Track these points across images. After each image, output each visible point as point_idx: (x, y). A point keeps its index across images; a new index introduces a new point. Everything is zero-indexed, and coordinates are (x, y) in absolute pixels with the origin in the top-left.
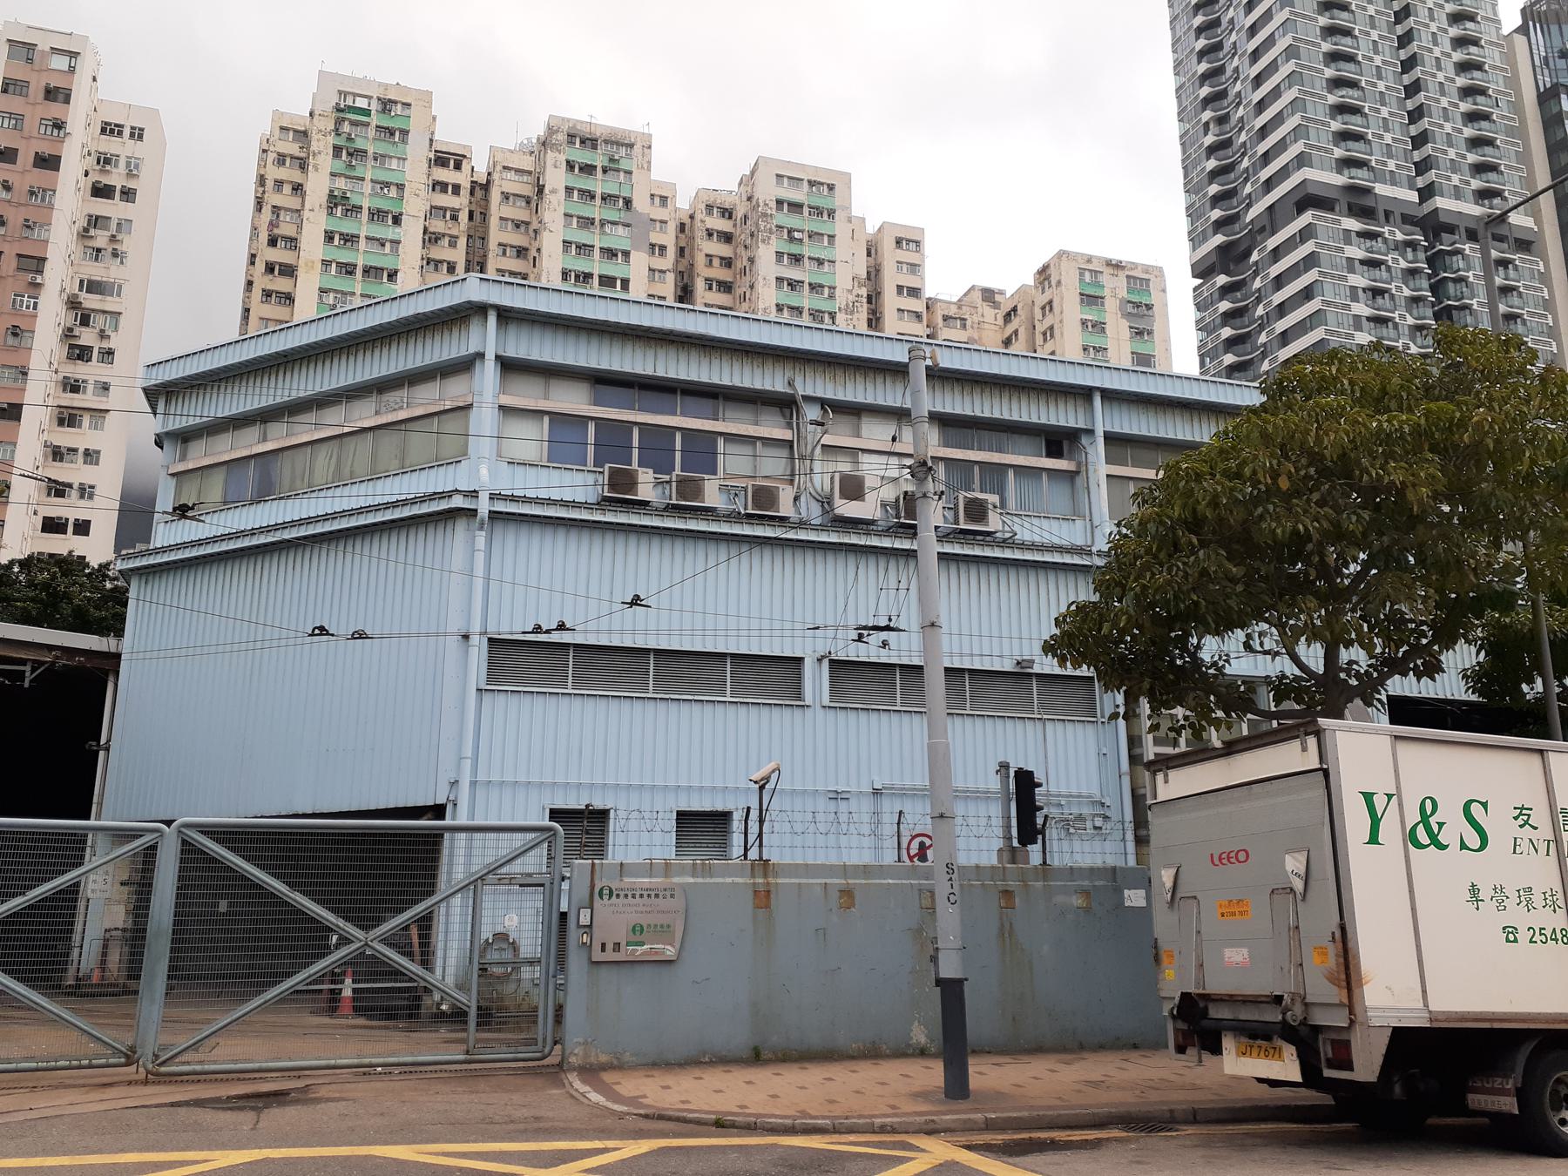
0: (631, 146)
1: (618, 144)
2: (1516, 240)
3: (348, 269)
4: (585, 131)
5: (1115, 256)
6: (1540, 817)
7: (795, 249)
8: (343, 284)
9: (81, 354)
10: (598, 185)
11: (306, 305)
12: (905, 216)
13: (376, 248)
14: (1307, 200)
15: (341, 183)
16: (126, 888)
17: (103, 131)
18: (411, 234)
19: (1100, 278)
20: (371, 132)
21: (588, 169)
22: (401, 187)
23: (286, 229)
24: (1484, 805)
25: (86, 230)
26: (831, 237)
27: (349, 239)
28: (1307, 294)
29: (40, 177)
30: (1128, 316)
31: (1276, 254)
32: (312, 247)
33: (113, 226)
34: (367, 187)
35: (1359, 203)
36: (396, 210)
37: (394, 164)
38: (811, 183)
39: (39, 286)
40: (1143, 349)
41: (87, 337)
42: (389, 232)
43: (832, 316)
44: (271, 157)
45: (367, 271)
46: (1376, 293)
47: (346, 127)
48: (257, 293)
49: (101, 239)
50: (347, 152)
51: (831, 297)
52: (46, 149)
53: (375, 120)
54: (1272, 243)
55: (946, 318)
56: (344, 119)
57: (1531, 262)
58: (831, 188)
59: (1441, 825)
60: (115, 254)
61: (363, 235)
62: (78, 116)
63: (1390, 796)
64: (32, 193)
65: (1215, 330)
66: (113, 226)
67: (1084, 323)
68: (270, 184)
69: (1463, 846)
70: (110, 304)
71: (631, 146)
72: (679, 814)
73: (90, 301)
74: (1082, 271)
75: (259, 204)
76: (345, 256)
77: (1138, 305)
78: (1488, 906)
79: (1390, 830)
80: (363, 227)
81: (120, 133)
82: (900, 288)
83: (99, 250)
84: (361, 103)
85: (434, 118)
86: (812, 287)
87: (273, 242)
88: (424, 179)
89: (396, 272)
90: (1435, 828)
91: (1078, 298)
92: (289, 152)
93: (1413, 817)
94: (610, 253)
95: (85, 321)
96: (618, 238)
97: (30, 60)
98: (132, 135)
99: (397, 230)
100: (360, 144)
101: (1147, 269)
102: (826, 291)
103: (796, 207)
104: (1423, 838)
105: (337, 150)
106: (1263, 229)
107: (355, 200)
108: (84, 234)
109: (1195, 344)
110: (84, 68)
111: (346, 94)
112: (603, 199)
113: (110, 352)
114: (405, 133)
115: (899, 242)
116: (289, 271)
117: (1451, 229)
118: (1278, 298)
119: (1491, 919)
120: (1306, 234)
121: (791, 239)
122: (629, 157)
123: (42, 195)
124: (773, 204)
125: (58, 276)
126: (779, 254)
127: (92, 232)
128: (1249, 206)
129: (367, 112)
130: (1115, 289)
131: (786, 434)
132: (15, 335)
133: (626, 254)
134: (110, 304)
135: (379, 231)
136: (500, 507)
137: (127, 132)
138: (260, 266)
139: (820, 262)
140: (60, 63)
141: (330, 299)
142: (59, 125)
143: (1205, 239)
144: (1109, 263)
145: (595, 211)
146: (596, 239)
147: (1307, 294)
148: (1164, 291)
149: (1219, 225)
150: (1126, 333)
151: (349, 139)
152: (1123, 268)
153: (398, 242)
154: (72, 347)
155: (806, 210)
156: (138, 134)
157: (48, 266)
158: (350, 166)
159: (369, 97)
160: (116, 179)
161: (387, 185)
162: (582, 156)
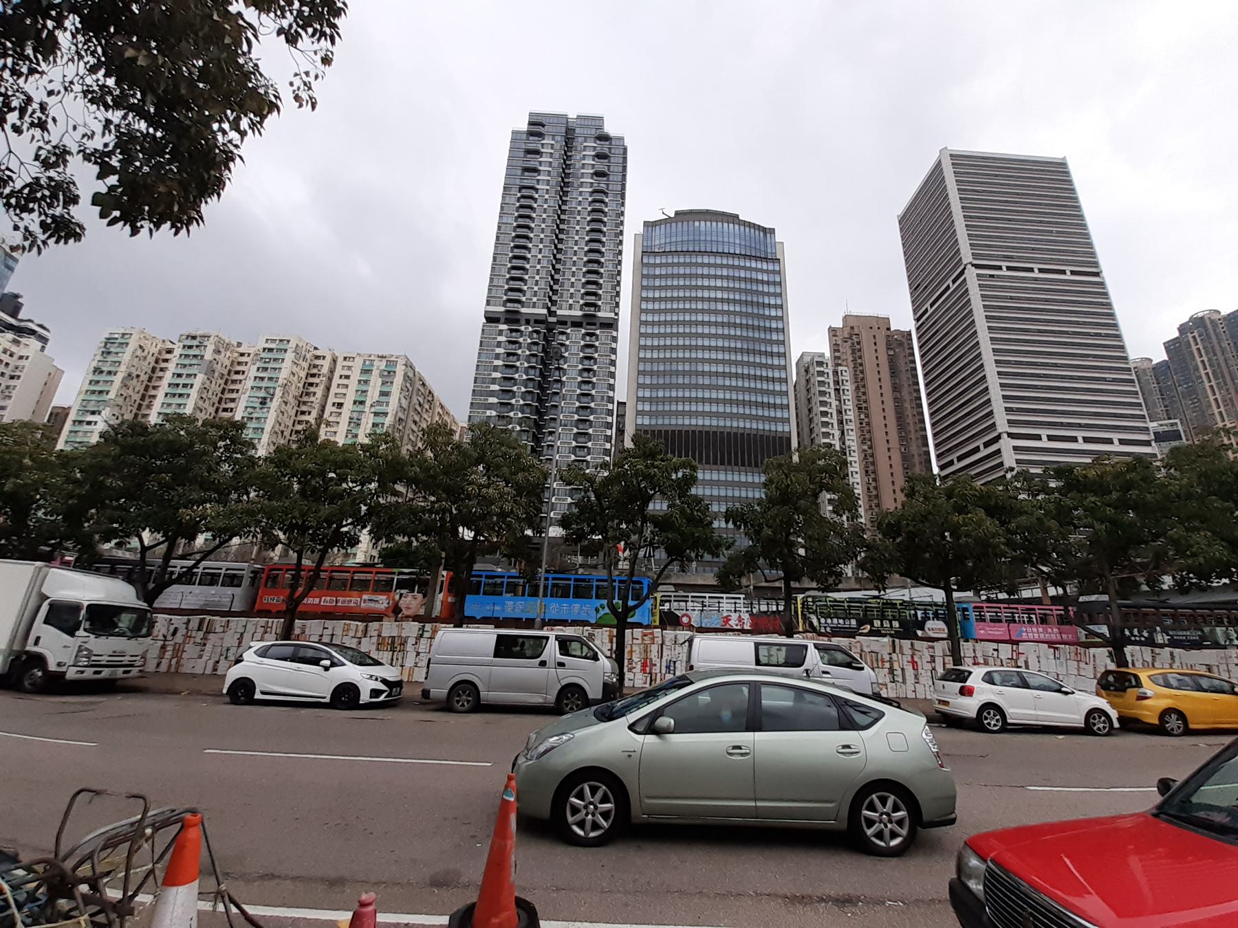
10: (191, 352)
21: (190, 347)
30: (381, 376)
35: (512, 318)
46: (509, 354)
86: (270, 379)
94: (189, 376)
103: (271, 350)
115: (345, 359)
117: (565, 323)
145: (187, 362)
162: (189, 342)
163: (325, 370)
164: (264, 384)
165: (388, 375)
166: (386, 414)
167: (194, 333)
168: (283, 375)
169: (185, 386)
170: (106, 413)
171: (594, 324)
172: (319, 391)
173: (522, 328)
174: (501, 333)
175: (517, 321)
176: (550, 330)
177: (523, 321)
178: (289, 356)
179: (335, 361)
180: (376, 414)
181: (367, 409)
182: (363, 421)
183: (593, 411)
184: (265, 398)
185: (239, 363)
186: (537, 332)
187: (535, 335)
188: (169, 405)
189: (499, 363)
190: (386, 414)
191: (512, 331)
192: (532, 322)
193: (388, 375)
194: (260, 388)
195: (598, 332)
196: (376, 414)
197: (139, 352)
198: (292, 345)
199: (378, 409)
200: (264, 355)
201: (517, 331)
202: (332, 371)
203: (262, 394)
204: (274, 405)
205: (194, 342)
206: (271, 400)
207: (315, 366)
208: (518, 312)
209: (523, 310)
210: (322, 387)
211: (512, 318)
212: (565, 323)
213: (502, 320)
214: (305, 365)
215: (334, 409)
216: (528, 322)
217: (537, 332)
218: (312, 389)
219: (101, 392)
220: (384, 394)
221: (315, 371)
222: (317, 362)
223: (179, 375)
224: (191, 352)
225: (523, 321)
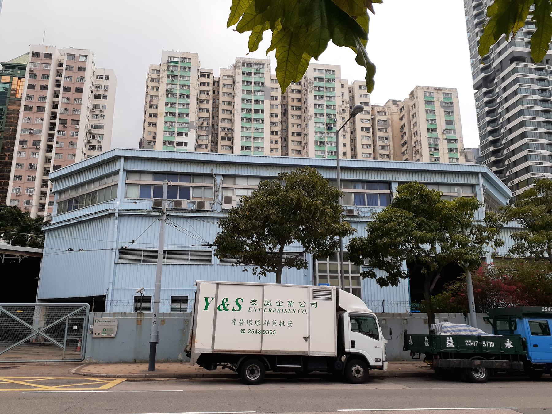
0: (264, 64)
1: (259, 64)
3: (173, 114)
4: (248, 61)
5: (438, 86)
6: (259, 303)
7: (321, 94)
8: (172, 119)
9: (92, 148)
10: (253, 79)
11: (79, 157)
13: (181, 107)
14: (514, 58)
15: (170, 86)
16: (44, 317)
17: (97, 78)
18: (193, 101)
19: (433, 94)
20: (179, 69)
21: (249, 74)
22: (189, 86)
23: (154, 102)
24: (242, 300)
25: (93, 109)
26: (334, 88)
27: (173, 104)
28: (515, 93)
29: (77, 95)
30: (443, 107)
31: (504, 79)
32: (162, 108)
33: (101, 107)
34: (178, 87)
36: (187, 94)
37: (187, 79)
38: (326, 70)
39: (78, 129)
40: (450, 119)
41: (94, 143)
42: (185, 101)
43: (335, 115)
44: (150, 79)
45: (179, 114)
46: (543, 90)
47: (171, 68)
48: (147, 124)
49: (97, 112)
50: (172, 76)
51: (334, 109)
52: (79, 86)
53: (180, 65)
54: (502, 75)
55: (378, 112)
56: (170, 65)
58: (333, 71)
59: (228, 305)
60: (102, 116)
61: (177, 103)
62: (88, 74)
63: (213, 298)
64: (75, 100)
65: (482, 108)
66: (101, 107)
67: (427, 111)
68: (150, 88)
69: (233, 310)
70: (100, 132)
71: (264, 64)
72: (172, 297)
73: (95, 131)
74: (425, 92)
75: (147, 94)
76: (172, 110)
77: (447, 103)
78: (238, 324)
79: (212, 306)
80: (177, 100)
81: (102, 78)
83: (97, 115)
84: (176, 60)
85: (200, 62)
86: (328, 106)
87: (151, 107)
88: (196, 82)
89: (188, 114)
90: (226, 306)
91: (424, 102)
92: (154, 79)
93: (220, 302)
94: (257, 102)
95: (93, 138)
96: (260, 96)
97: (73, 59)
98: (106, 78)
99: (188, 100)
100: (175, 73)
101: (450, 90)
102: (332, 107)
103: (321, 79)
104: (222, 308)
105: (168, 76)
106: (498, 70)
107: (174, 91)
108: (92, 111)
109: (476, 114)
110: (90, 59)
111: (171, 57)
112: (255, 83)
113: (101, 147)
114: (189, 68)
116: (155, 116)
118: (505, 95)
119: (238, 327)
120: (514, 71)
121: (320, 90)
122: (263, 68)
123: (78, 100)
124: (313, 79)
125: (84, 126)
126: (315, 96)
127: (95, 110)
128: (493, 62)
129: (177, 63)
130: (438, 98)
131: (212, 185)
132: (72, 144)
133: (263, 101)
134: (100, 132)
135: (183, 101)
136: (122, 212)
137: (104, 77)
138: (147, 115)
139: (330, 97)
140: (82, 59)
141: (168, 124)
142: (82, 78)
143: (478, 75)
144: (435, 89)
145: (252, 88)
146: (252, 97)
147: (515, 93)
148: (457, 97)
149: (483, 70)
151: (172, 72)
152: (441, 90)
153: (189, 104)
154: (90, 146)
155: (324, 80)
156: (107, 78)
157: (80, 122)
158: (173, 81)
159: (178, 58)
160: (101, 92)
161: (185, 86)
162: (247, 70)
168: (338, 102)
170: (192, 134)
177: (545, 61)
178: (337, 85)
180: (448, 140)
181: (440, 136)
182: (440, 146)
194: (322, 115)
196: (448, 140)
200: (318, 84)
201: (541, 69)
203: (326, 120)
215: (364, 133)
223: (248, 101)
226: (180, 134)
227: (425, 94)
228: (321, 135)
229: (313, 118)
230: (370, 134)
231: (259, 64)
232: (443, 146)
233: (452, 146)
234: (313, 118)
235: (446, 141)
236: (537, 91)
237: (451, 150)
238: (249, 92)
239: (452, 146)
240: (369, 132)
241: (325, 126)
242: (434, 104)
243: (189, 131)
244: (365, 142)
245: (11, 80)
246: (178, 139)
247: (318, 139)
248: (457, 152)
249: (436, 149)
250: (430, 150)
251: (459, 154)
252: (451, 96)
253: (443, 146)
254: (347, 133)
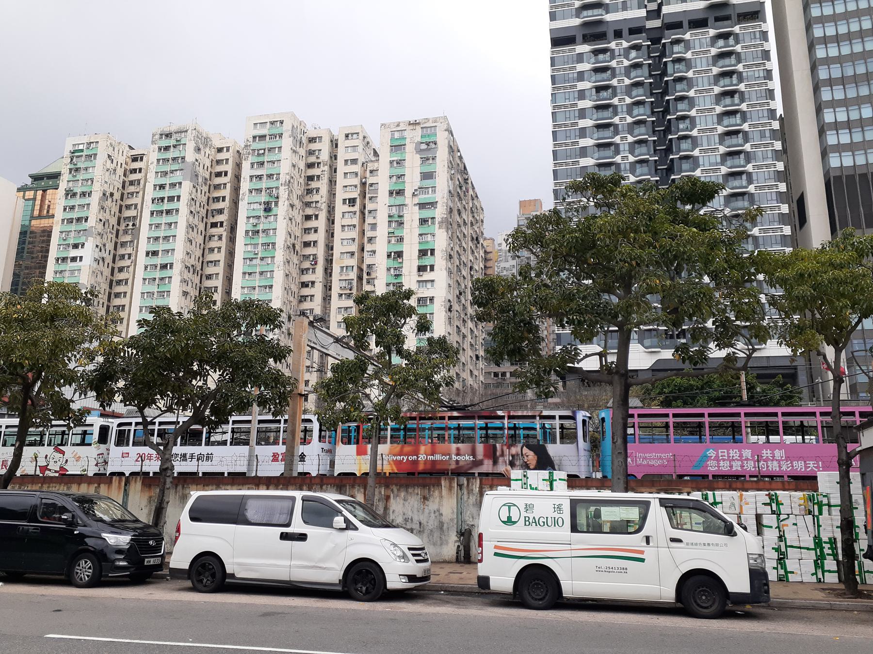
0: (186, 131)
1: (181, 132)
2: (739, 15)
5: (412, 120)
7: (260, 159)
10: (170, 154)
12: (350, 123)
19: (406, 134)
21: (167, 148)
26: (280, 148)
30: (419, 151)
35: (594, 33)
38: (272, 123)
43: (277, 188)
46: (599, 89)
47: (74, 160)
51: (278, 179)
55: (371, 172)
57: (753, 27)
58: (282, 122)
67: (391, 162)
71: (186, 131)
77: (428, 144)
82: (346, 161)
84: (81, 147)
86: (270, 176)
91: (389, 149)
94: (173, 185)
96: (177, 177)
105: (71, 170)
115: (347, 136)
117: (676, 25)
121: (259, 155)
124: (251, 140)
126: (252, 164)
129: (82, 151)
130: (414, 136)
145: (167, 168)
150: (419, 162)
152: (419, 124)
155: (268, 137)
162: (165, 143)
163: (325, 156)
164: (264, 184)
165: (427, 150)
166: (433, 204)
167: (167, 130)
168: (284, 169)
169: (171, 199)
171: (727, 18)
172: (322, 185)
173: (613, 45)
174: (580, 58)
175: (601, 37)
176: (656, 41)
177: (611, 34)
178: (287, 143)
179: (334, 144)
180: (422, 206)
182: (406, 219)
183: (749, 158)
184: (267, 203)
185: (219, 162)
186: (636, 47)
187: (633, 54)
188: (158, 226)
189: (586, 104)
190: (433, 204)
191: (596, 52)
192: (625, 32)
193: (427, 150)
194: (259, 191)
195: (737, 29)
196: (422, 206)
197: (109, 165)
198: (287, 128)
199: (423, 198)
201: (604, 51)
202: (334, 157)
203: (264, 198)
204: (282, 210)
205: (169, 140)
206: (276, 204)
207: (311, 153)
208: (600, 22)
209: (609, 17)
210: (325, 180)
211: (594, 33)
212: (676, 25)
213: (579, 38)
214: (302, 152)
215: (346, 208)
216: (618, 34)
217: (636, 47)
218: (314, 185)
219: (79, 220)
220: (427, 176)
221: (312, 159)
222: (313, 146)
223: (162, 187)
224: (170, 154)
225: (611, 34)
226: (76, 246)
227: (393, 135)
228: (255, 221)
229: (246, 197)
230: (357, 208)
231: (181, 132)
232: (412, 215)
233: (427, 214)
234: (246, 197)
235: (417, 207)
236: (587, 93)
237: (423, 221)
238: (165, 174)
239: (427, 214)
240: (353, 206)
241: (262, 207)
242: (404, 149)
243: (86, 240)
244: (346, 222)
245: (35, 195)
246: (73, 253)
247: (250, 228)
248: (433, 223)
249: (401, 224)
250: (390, 226)
251: (437, 225)
252: (435, 130)
253: (412, 215)
254: (322, 210)
